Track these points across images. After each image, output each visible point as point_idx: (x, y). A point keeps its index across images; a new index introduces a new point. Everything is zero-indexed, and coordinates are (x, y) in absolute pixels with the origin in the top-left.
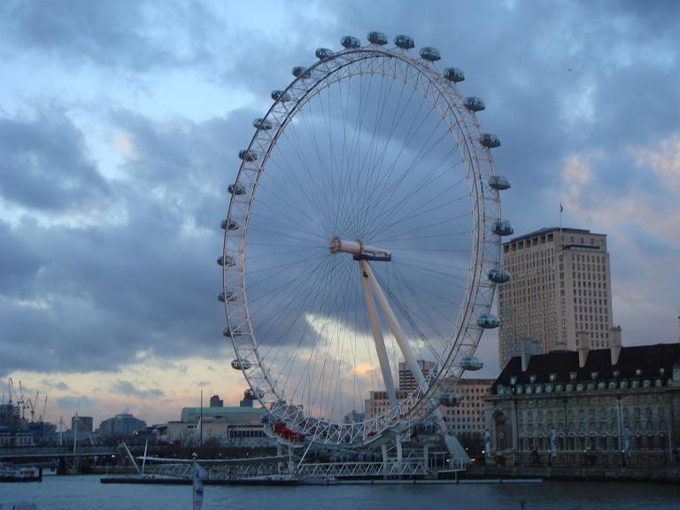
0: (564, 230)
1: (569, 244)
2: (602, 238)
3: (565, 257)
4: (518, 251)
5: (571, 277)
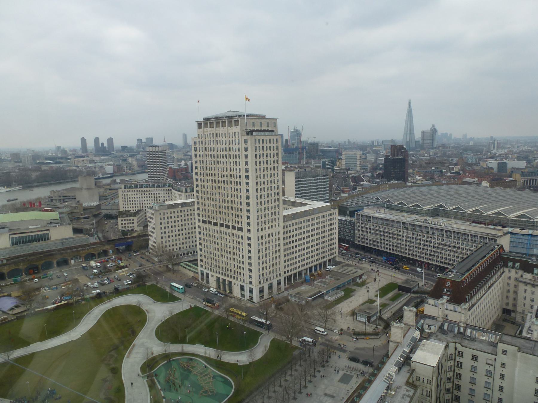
0: (249, 116)
1: (252, 129)
2: (274, 121)
3: (249, 142)
4: (209, 129)
5: (254, 158)
